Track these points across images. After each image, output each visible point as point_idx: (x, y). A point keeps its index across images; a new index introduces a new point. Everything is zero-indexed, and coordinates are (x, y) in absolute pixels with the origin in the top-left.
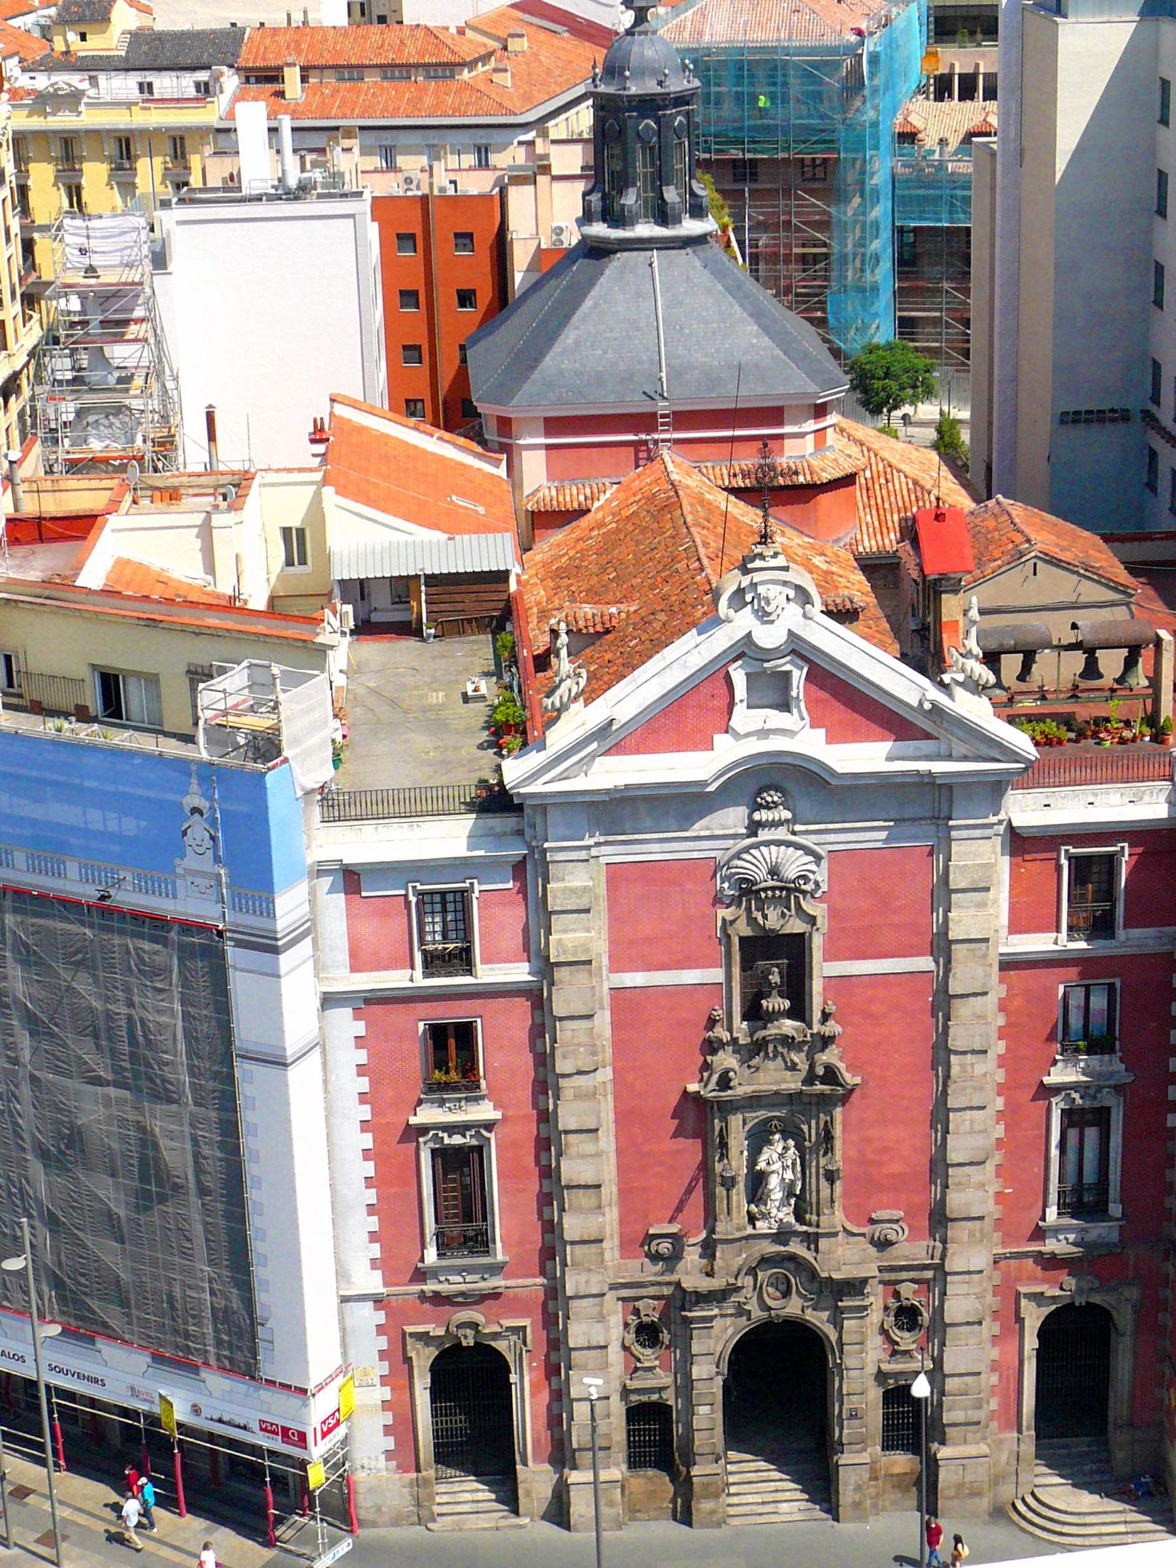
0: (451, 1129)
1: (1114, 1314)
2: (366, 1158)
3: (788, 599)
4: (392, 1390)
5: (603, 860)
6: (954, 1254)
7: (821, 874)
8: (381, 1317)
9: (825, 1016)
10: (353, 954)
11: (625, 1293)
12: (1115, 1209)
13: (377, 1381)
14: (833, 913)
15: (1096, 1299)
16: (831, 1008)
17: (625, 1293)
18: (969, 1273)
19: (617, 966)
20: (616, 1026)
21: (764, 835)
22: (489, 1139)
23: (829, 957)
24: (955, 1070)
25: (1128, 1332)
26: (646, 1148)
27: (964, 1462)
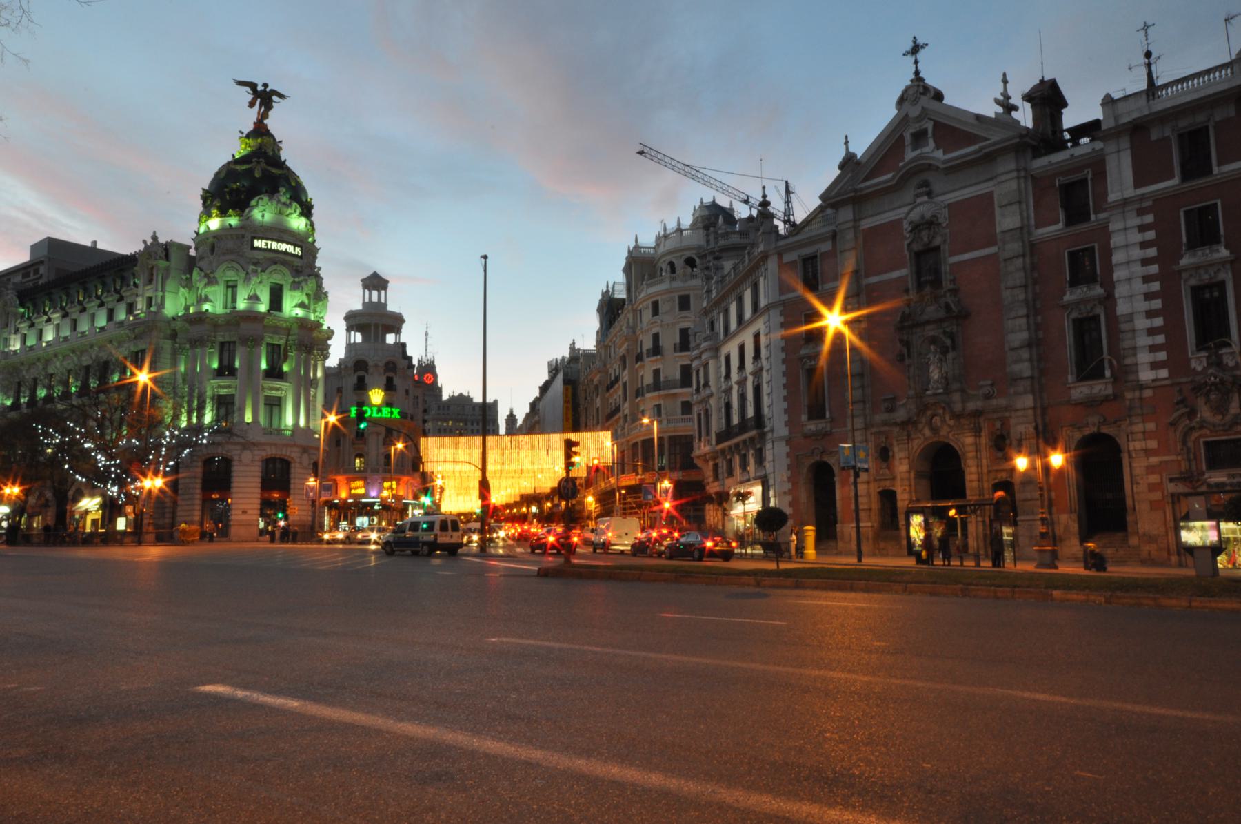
1: (1117, 439)
8: (787, 449)
10: (780, 289)
18: (1024, 409)
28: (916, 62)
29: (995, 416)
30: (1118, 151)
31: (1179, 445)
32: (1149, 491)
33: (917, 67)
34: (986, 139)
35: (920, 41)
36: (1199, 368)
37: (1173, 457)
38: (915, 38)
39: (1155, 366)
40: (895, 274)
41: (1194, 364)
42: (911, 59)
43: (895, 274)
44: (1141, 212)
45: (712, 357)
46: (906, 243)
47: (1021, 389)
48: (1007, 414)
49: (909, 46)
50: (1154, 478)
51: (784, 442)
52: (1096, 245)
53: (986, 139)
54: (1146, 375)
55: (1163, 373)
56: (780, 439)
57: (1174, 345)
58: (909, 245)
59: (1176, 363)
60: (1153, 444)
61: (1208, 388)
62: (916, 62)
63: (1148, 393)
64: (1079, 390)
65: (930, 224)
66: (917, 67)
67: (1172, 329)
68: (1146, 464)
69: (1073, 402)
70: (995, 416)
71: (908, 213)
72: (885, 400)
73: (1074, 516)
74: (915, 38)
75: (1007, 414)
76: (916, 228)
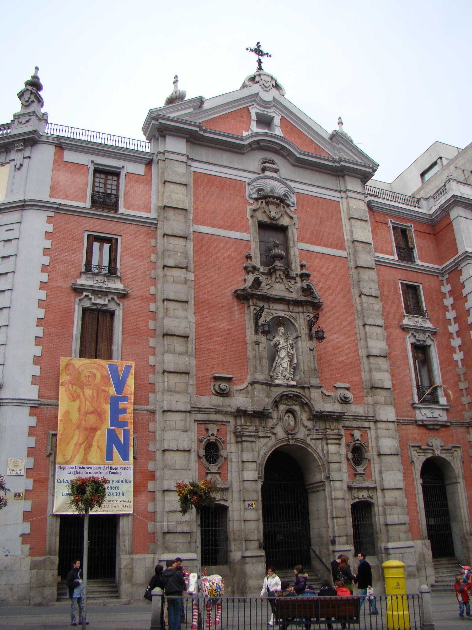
0: (96, 292)
1: (452, 464)
2: (40, 306)
3: (273, 86)
4: (34, 481)
5: (193, 169)
6: (380, 409)
7: (293, 199)
8: (33, 421)
9: (302, 266)
11: (200, 417)
12: (443, 401)
13: (23, 472)
14: (300, 220)
15: (443, 456)
16: (303, 263)
17: (200, 417)
18: (388, 421)
19: (196, 222)
20: (196, 252)
21: (268, 173)
22: (119, 305)
23: (300, 240)
24: (365, 305)
25: (461, 476)
26: (211, 325)
27: (402, 550)
28: (259, 61)
29: (355, 424)
42: (256, 57)
47: (382, 399)
48: (366, 424)
49: (254, 46)
51: (27, 410)
52: (421, 285)
56: (20, 402)
62: (259, 61)
64: (423, 411)
69: (420, 423)
70: (355, 424)
72: (216, 379)
73: (428, 542)
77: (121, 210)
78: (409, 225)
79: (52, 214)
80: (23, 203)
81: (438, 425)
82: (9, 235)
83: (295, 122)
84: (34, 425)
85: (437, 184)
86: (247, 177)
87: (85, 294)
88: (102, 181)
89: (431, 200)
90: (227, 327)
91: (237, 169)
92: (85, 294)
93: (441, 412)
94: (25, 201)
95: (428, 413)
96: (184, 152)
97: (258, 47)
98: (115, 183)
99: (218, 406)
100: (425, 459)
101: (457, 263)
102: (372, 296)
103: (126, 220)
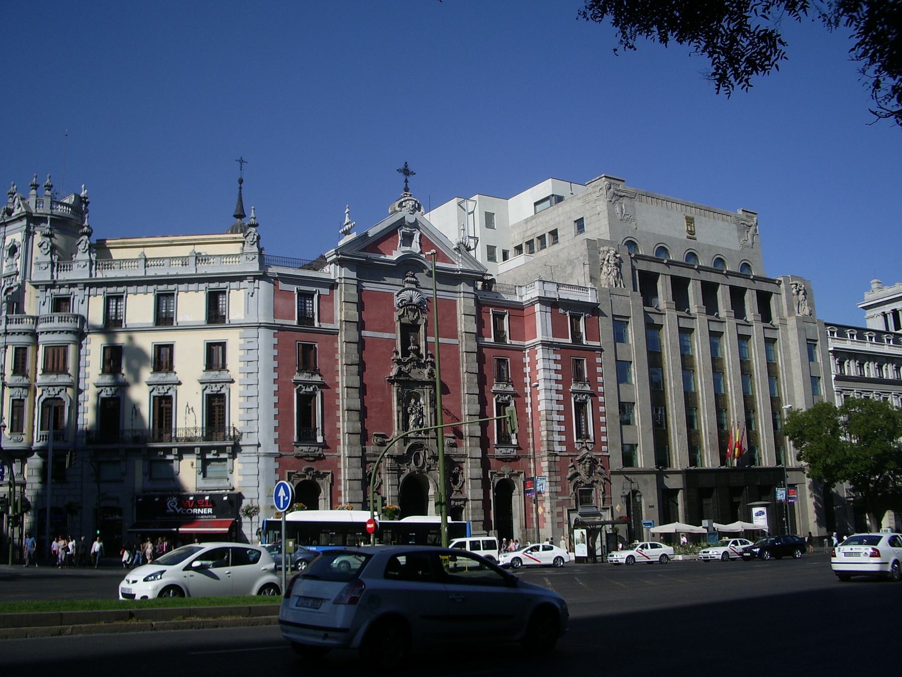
8: (277, 465)
26: (372, 400)
28: (406, 181)
30: (546, 312)
31: (571, 491)
32: (558, 516)
33: (406, 185)
34: (453, 263)
35: (411, 168)
36: (579, 449)
37: (568, 498)
38: (406, 163)
39: (561, 443)
40: (387, 335)
41: (576, 446)
42: (402, 177)
43: (387, 335)
44: (555, 352)
45: (75, 343)
46: (396, 316)
48: (462, 460)
49: (402, 166)
50: (559, 509)
51: (273, 459)
53: (453, 263)
54: (558, 448)
55: (564, 448)
57: (568, 433)
58: (400, 317)
59: (569, 444)
60: (559, 489)
61: (586, 460)
62: (406, 181)
63: (558, 459)
65: (420, 307)
66: (406, 185)
67: (567, 423)
68: (556, 501)
71: (400, 293)
74: (406, 163)
75: (462, 460)
76: (407, 305)
77: (316, 324)
78: (505, 311)
79: (276, 331)
80: (258, 325)
81: (509, 458)
82: (250, 346)
83: (430, 236)
84: (278, 467)
85: (547, 219)
86: (395, 290)
87: (299, 385)
88: (303, 301)
89: (524, 288)
90: (382, 401)
91: (389, 284)
92: (299, 385)
93: (512, 450)
94: (260, 323)
95: (504, 450)
96: (355, 277)
97: (406, 167)
98: (311, 302)
99: (376, 452)
100: (499, 480)
101: (535, 346)
102: (473, 373)
103: (320, 332)
